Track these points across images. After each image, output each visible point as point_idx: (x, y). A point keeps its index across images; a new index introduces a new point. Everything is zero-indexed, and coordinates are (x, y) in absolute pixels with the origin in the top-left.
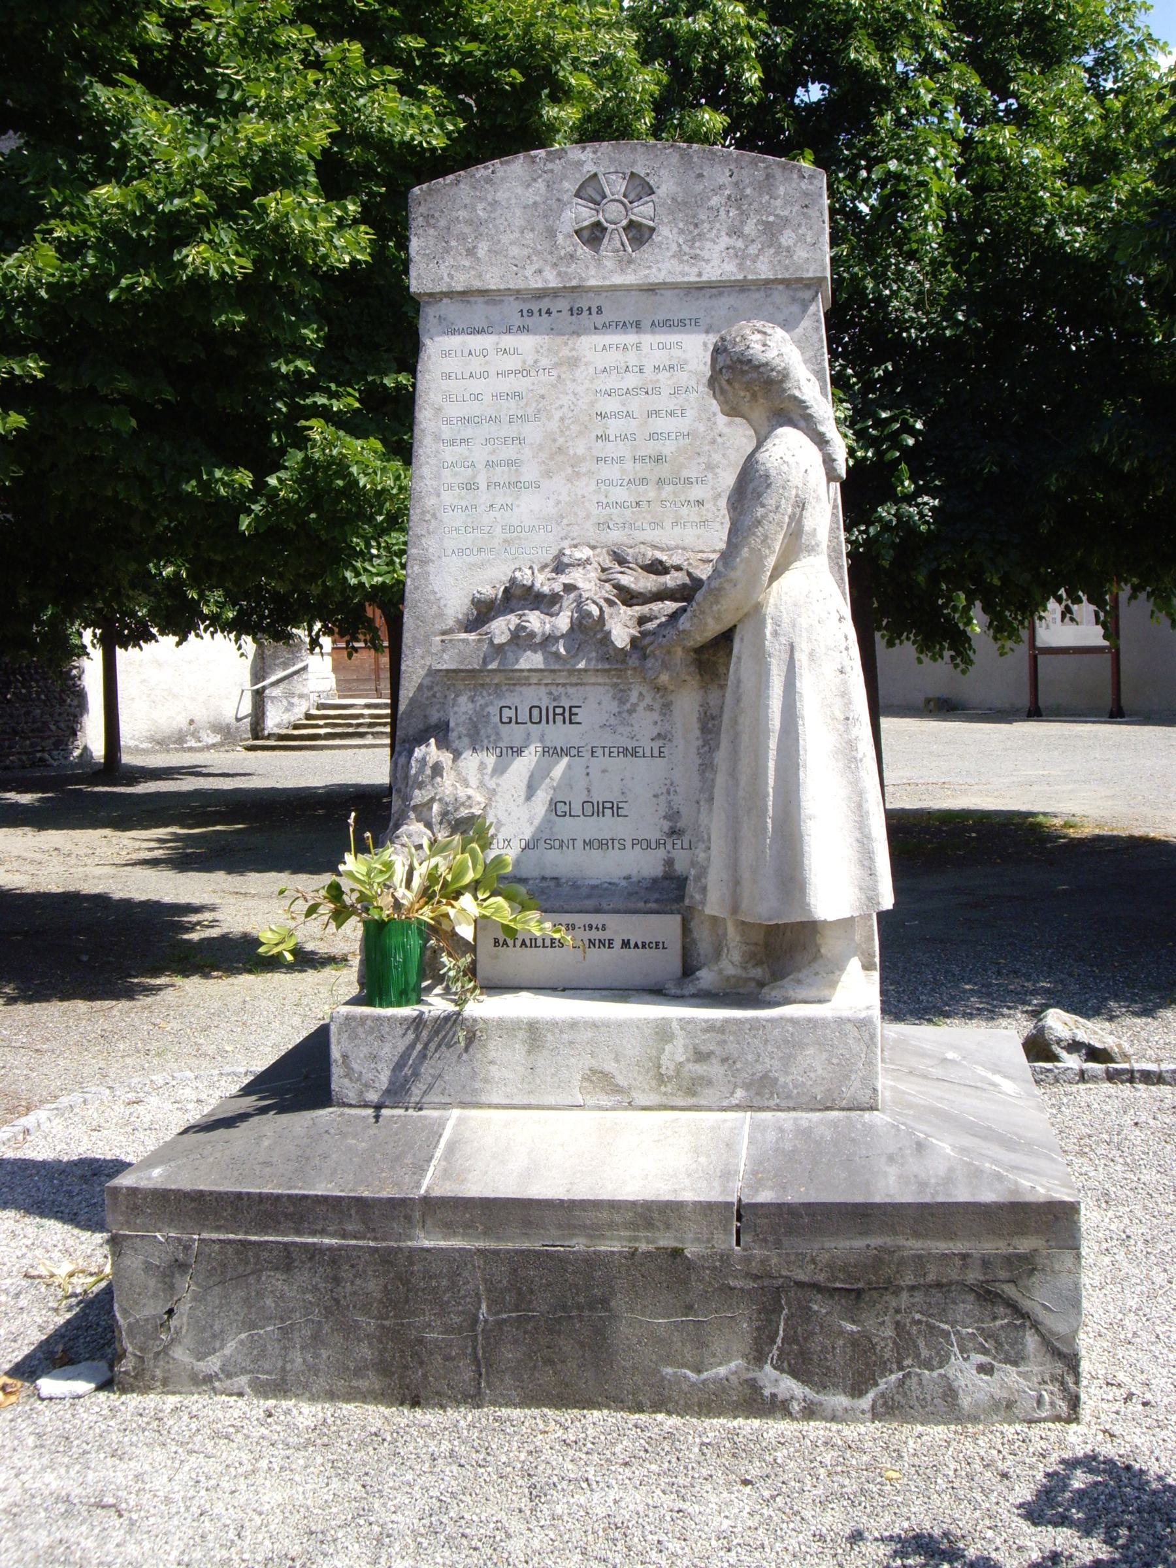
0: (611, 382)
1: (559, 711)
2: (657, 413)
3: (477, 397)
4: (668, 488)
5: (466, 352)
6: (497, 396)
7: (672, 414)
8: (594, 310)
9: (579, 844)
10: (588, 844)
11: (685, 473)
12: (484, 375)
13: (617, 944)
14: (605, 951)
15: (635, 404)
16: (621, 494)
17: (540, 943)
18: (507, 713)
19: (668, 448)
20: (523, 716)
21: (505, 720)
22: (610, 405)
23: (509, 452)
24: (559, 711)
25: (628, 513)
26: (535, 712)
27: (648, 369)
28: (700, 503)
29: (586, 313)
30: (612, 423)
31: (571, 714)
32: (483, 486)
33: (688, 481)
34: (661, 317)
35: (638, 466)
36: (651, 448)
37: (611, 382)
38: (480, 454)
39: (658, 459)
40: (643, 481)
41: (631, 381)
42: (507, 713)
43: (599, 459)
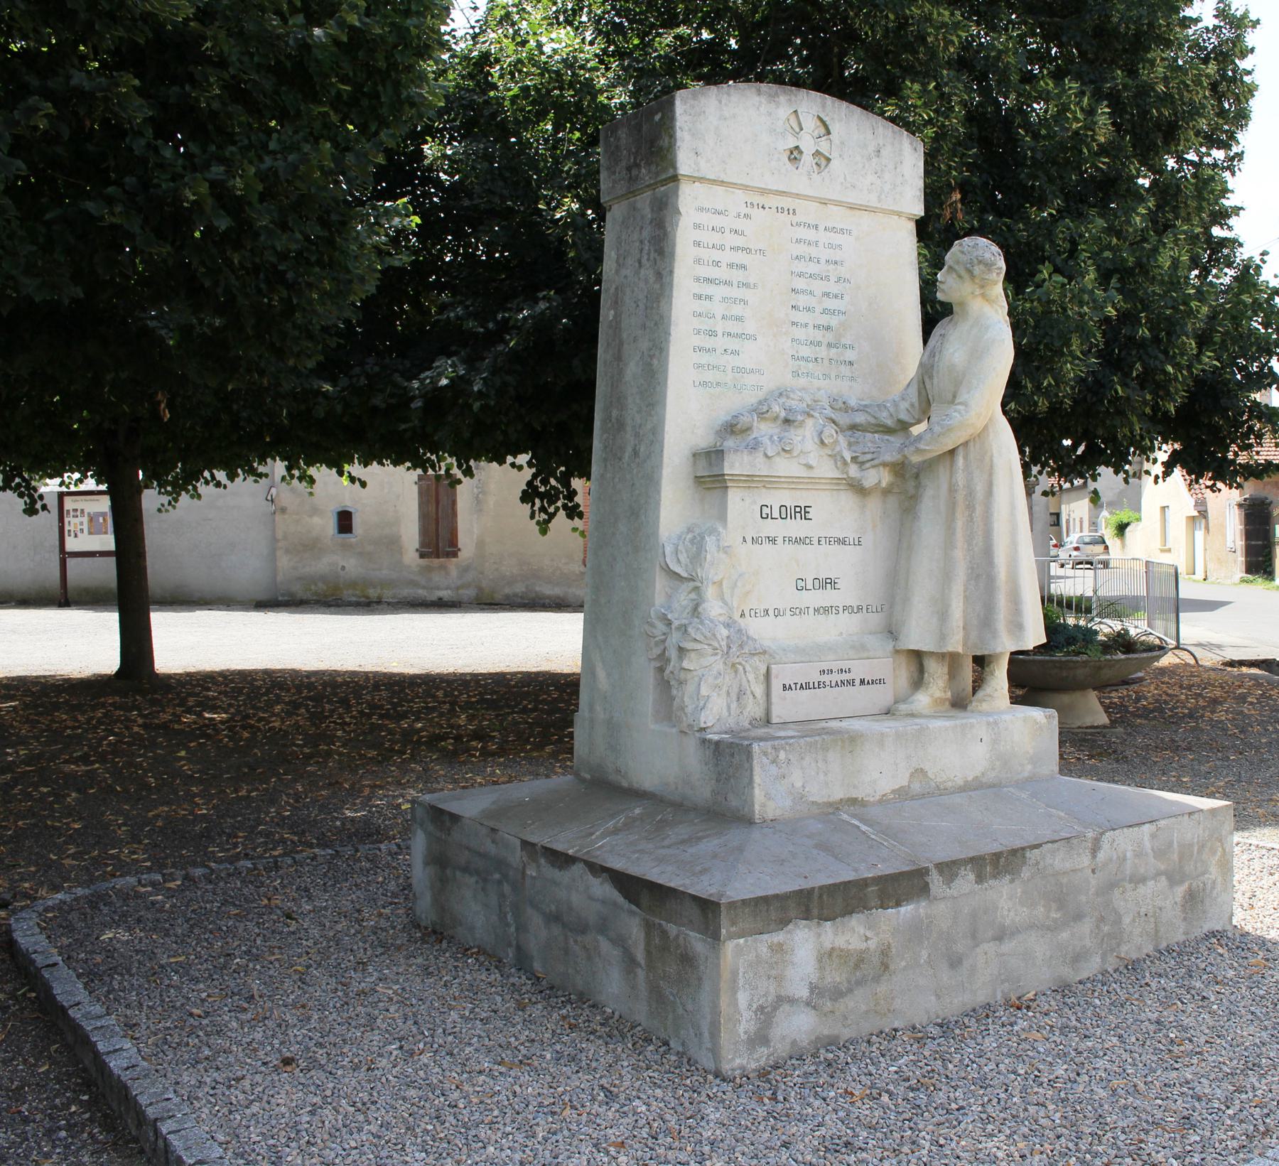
0: (800, 267)
2: (826, 294)
3: (717, 264)
4: (834, 351)
6: (731, 266)
7: (836, 297)
9: (811, 610)
10: (817, 610)
11: (843, 341)
12: (722, 248)
13: (857, 682)
14: (850, 687)
16: (806, 351)
18: (766, 510)
19: (834, 321)
20: (776, 514)
22: (801, 284)
23: (737, 310)
25: (811, 365)
27: (823, 261)
28: (851, 363)
30: (801, 296)
32: (720, 334)
33: (844, 346)
36: (824, 320)
37: (800, 267)
38: (718, 309)
39: (828, 328)
40: (819, 344)
41: (812, 268)
42: (766, 510)
43: (793, 323)
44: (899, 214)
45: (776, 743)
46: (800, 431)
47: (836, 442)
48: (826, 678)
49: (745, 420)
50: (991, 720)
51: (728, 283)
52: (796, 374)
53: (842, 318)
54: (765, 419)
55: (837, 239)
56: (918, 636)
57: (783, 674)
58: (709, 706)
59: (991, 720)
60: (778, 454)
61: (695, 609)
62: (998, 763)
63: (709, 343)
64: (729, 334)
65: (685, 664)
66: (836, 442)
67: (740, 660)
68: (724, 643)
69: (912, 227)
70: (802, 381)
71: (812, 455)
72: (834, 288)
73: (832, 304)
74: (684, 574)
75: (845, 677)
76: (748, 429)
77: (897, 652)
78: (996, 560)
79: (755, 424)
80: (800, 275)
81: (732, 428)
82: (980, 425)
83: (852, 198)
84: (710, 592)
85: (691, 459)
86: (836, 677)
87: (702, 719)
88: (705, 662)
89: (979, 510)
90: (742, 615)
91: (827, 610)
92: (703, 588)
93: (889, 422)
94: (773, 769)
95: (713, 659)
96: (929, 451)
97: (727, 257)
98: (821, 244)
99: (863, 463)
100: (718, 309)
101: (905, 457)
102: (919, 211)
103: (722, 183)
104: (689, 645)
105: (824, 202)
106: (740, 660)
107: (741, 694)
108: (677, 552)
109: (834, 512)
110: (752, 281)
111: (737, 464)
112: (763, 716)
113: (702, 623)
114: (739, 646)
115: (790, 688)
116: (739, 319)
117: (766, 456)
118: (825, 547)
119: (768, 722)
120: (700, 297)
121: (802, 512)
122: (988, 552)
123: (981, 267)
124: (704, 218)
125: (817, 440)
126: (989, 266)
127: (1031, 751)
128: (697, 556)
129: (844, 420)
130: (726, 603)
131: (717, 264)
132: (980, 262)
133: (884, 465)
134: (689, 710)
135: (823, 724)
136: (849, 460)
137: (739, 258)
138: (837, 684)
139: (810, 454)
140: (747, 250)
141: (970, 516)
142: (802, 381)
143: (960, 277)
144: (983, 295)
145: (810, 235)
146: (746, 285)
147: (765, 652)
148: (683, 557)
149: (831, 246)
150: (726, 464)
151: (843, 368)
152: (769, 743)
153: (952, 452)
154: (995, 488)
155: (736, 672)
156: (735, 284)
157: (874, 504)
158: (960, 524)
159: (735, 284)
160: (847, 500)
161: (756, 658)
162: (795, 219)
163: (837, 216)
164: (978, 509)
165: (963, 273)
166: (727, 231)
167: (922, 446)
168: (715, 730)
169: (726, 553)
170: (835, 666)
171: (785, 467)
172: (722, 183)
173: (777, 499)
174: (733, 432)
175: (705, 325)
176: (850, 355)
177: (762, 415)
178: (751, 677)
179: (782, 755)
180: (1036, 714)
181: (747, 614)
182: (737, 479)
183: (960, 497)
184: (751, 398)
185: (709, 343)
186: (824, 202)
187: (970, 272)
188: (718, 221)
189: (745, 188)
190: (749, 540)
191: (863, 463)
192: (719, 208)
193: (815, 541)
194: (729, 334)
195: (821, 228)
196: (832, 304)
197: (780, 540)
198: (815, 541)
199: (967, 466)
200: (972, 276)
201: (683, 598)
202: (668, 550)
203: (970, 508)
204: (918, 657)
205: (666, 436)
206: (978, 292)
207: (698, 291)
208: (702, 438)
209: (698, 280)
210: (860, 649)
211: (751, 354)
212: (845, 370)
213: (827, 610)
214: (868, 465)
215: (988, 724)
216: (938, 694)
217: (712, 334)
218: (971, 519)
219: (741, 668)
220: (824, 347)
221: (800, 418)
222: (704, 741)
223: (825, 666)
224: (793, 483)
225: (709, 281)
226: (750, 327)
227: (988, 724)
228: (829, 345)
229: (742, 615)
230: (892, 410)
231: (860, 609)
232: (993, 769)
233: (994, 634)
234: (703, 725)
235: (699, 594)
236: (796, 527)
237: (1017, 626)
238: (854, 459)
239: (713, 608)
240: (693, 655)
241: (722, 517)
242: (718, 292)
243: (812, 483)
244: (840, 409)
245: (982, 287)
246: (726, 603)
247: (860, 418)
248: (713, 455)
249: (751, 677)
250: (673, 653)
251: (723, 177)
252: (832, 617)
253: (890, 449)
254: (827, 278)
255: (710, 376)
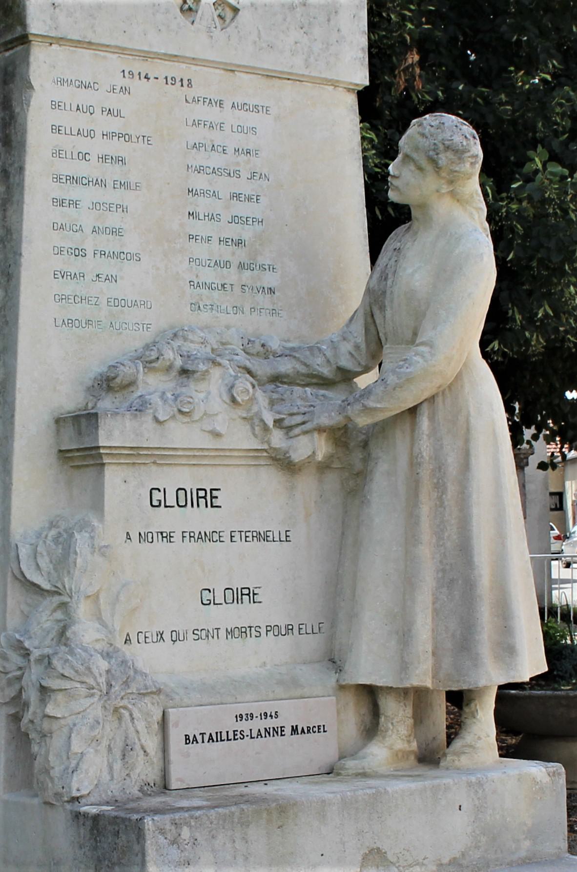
0: (200, 158)
1: (201, 493)
2: (236, 196)
3: (84, 156)
4: (247, 273)
5: (74, 108)
6: (103, 158)
7: (249, 199)
8: (185, 83)
9: (222, 633)
10: (230, 633)
11: (260, 260)
12: (91, 134)
13: (287, 731)
14: (278, 738)
15: (224, 186)
16: (209, 275)
17: (224, 737)
19: (247, 233)
21: (155, 503)
22: (200, 182)
23: (113, 220)
24: (201, 493)
25: (216, 294)
26: (181, 493)
27: (230, 150)
28: (271, 291)
29: (179, 84)
30: (201, 200)
31: (212, 497)
32: (90, 253)
33: (262, 267)
34: (239, 100)
35: (223, 246)
36: (234, 231)
37: (200, 158)
38: (88, 220)
39: (239, 243)
40: (227, 264)
41: (216, 160)
43: (191, 237)
44: (335, 84)
45: (177, 816)
46: (202, 386)
47: (253, 399)
48: (244, 726)
49: (126, 371)
50: (473, 779)
51: (100, 183)
52: (196, 307)
53: (258, 228)
54: (152, 369)
55: (250, 119)
56: (369, 666)
57: (184, 722)
58: (84, 766)
59: (473, 779)
60: (173, 417)
61: (62, 633)
62: (484, 839)
63: (74, 265)
64: (103, 254)
65: (50, 710)
66: (253, 399)
67: (125, 702)
68: (102, 680)
69: (352, 100)
70: (205, 317)
71: (220, 417)
72: (246, 187)
73: (243, 209)
74: (46, 586)
75: (270, 723)
76: (130, 385)
77: (342, 688)
78: (476, 559)
79: (141, 376)
80: (199, 170)
81: (108, 383)
82: (451, 374)
83: (268, 62)
84: (82, 610)
85: (53, 426)
86: (259, 724)
87: (75, 785)
88: (76, 706)
89: (452, 489)
90: (127, 641)
91: (244, 632)
92: (73, 605)
93: (326, 371)
94: (174, 853)
95: (87, 702)
96: (381, 410)
97: (98, 147)
98: (227, 127)
99: (290, 428)
100: (88, 220)
101: (349, 419)
102: (362, 78)
103: (89, 45)
104: (53, 683)
105: (231, 69)
106: (125, 702)
107: (127, 750)
108: (35, 554)
109: (252, 496)
110: (133, 179)
111: (116, 433)
112: (158, 780)
113: (72, 652)
114: (124, 684)
115: (195, 740)
116: (116, 232)
117: (156, 420)
118: (239, 545)
119: (165, 787)
120: (62, 203)
121: (208, 497)
122: (465, 548)
123: (449, 154)
124: (64, 94)
125: (226, 398)
126: (459, 153)
127: (529, 822)
128: (64, 561)
129: (263, 369)
130: (105, 625)
131: (84, 156)
132: (447, 148)
133: (320, 430)
134: (56, 772)
135: (242, 789)
136: (270, 424)
137: (115, 147)
138: (259, 734)
139: (218, 417)
140: (125, 137)
141: (440, 498)
142: (205, 317)
143: (420, 169)
144: (453, 194)
145: (211, 114)
146: (125, 185)
147: (159, 691)
148: (44, 562)
149: (241, 129)
150: (101, 432)
151: (260, 297)
152: (168, 817)
153: (413, 411)
154: (473, 461)
155: (120, 719)
156: (110, 183)
157: (307, 485)
158: (425, 509)
159: (110, 183)
160: (270, 479)
161: (147, 700)
162: (192, 93)
163: (249, 88)
164: (451, 487)
165: (424, 163)
166: (98, 111)
167: (371, 404)
168: (92, 799)
169: (103, 555)
170: (256, 709)
171: (181, 436)
172: (89, 45)
173: (172, 479)
174: (110, 389)
175: (69, 241)
176: (270, 279)
177: (149, 365)
178: (141, 725)
179: (186, 833)
180: (535, 769)
181: (134, 639)
182: (116, 452)
183: (425, 473)
184: (135, 341)
185: (74, 265)
186: (231, 69)
187: (433, 162)
188: (84, 97)
189: (121, 51)
190: (135, 536)
191: (290, 428)
192: (86, 79)
193: (226, 537)
194: (103, 254)
195: (227, 105)
196: (243, 209)
197: (177, 537)
198: (226, 537)
199: (434, 431)
200: (437, 168)
201: (46, 618)
202: (24, 552)
203: (440, 487)
204: (370, 694)
205: (19, 396)
206: (445, 189)
207: (58, 194)
208: (69, 399)
209: (58, 179)
210: (290, 685)
211: (133, 280)
212: (263, 300)
213: (244, 632)
214: (297, 431)
215: (470, 784)
216: (400, 745)
217: (79, 253)
218: (440, 503)
219: (126, 714)
220: (233, 269)
221: (202, 367)
222: (77, 815)
223: (243, 709)
224: (195, 457)
225: (73, 180)
226: (131, 243)
227: (470, 784)
228: (241, 266)
229: (127, 641)
230: (329, 354)
231: (289, 629)
232: (477, 847)
233: (476, 660)
234: (75, 794)
235: (67, 613)
236: (199, 518)
237: (507, 650)
238: (278, 423)
239: (87, 632)
240: (60, 697)
241: (98, 505)
242: (86, 195)
243: (219, 457)
244: (258, 354)
245: (451, 182)
246: (105, 625)
247: (286, 367)
248: (85, 420)
249: (141, 725)
250: (32, 695)
251: (90, 37)
252: (251, 641)
253: (328, 408)
254: (237, 174)
255: (76, 311)
